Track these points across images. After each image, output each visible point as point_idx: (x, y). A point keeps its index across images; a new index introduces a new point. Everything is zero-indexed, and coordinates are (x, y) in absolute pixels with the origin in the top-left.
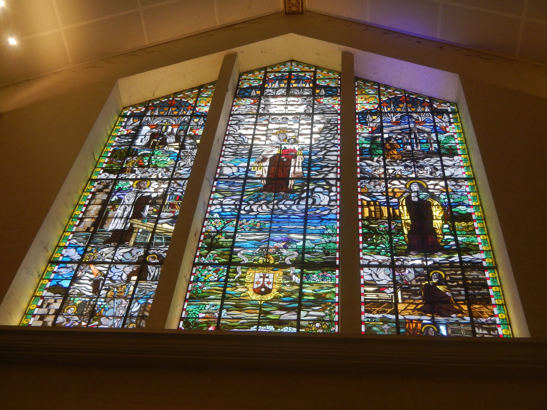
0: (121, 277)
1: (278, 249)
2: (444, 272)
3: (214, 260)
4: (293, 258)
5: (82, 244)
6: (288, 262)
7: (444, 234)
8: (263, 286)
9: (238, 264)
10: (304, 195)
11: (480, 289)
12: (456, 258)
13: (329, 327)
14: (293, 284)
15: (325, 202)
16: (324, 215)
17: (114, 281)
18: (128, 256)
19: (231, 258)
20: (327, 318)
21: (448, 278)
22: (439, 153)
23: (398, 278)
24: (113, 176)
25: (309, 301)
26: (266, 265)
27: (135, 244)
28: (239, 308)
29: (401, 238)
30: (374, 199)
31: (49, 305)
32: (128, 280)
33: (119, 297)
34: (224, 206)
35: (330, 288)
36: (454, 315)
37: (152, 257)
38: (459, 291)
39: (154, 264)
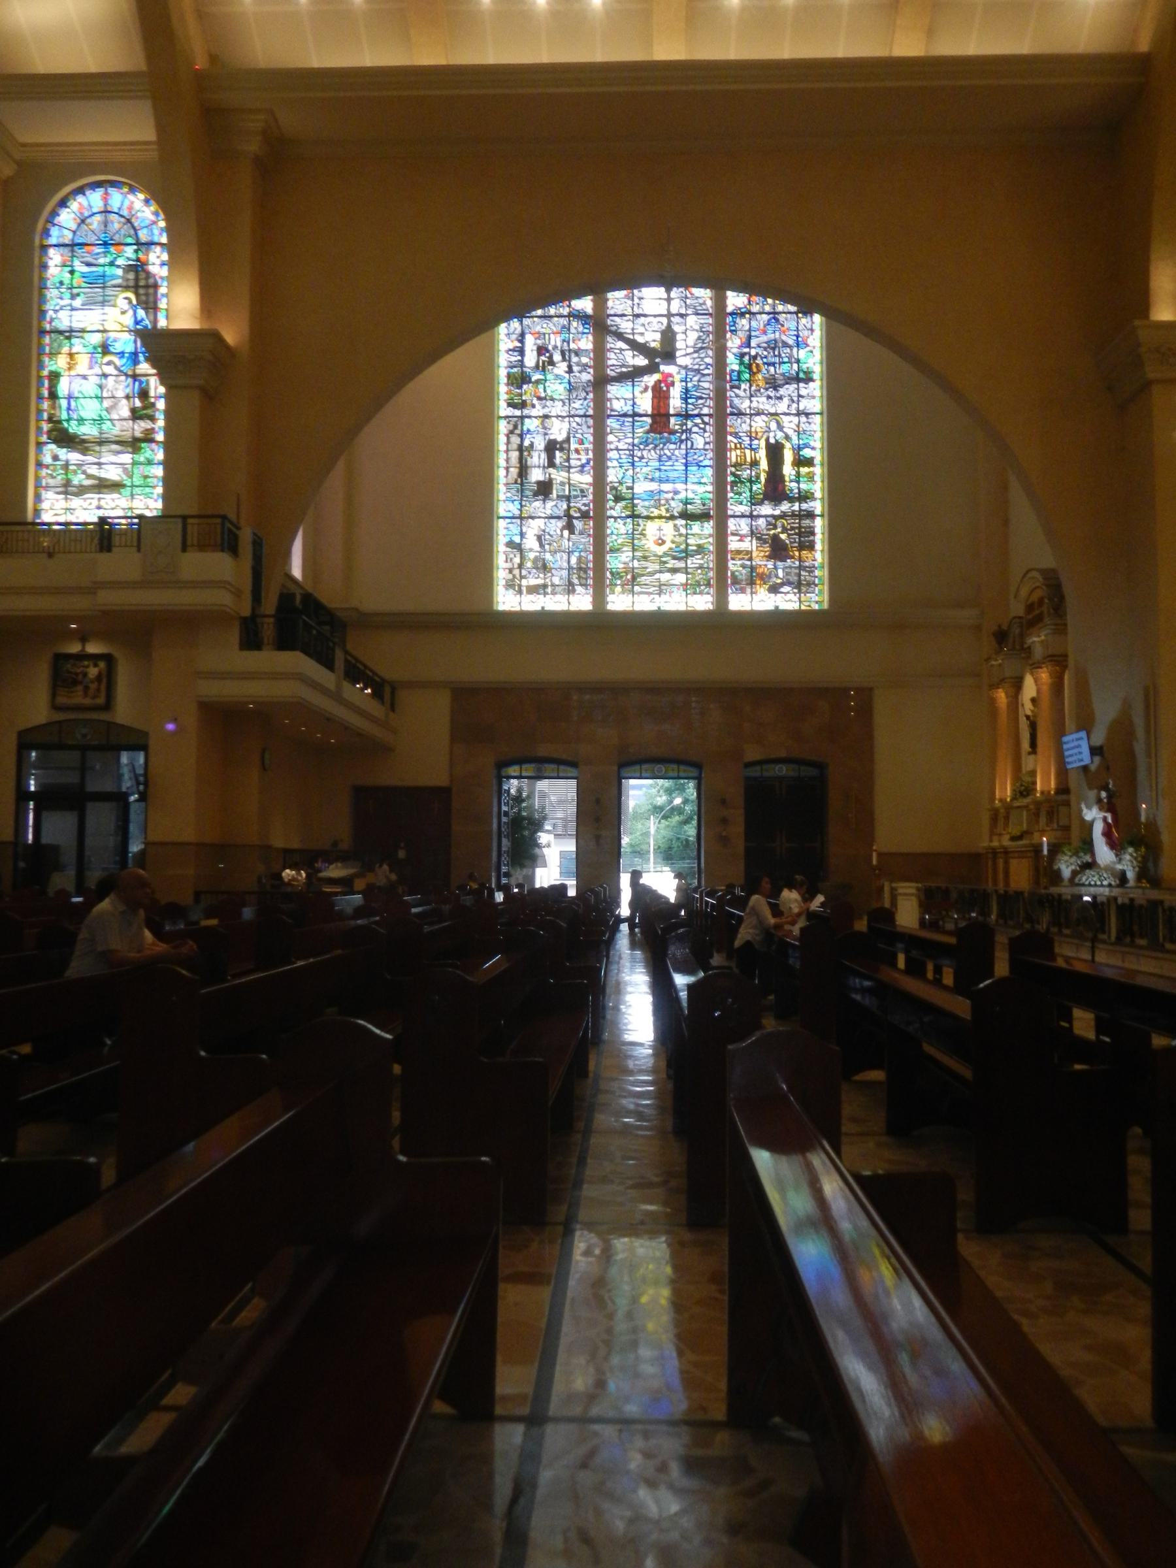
0: (555, 531)
1: (667, 500)
2: (786, 520)
3: (622, 512)
4: (679, 509)
5: (516, 498)
6: (676, 514)
7: (791, 481)
8: (660, 539)
9: (639, 516)
10: (684, 437)
11: (808, 537)
12: (796, 507)
13: (707, 573)
14: (681, 535)
15: (701, 446)
16: (701, 461)
17: (551, 536)
18: (555, 509)
19: (634, 511)
20: (706, 565)
21: (789, 527)
22: (797, 380)
23: (754, 528)
24: (518, 413)
25: (693, 551)
26: (660, 517)
27: (558, 496)
28: (645, 558)
29: (759, 486)
30: (740, 441)
31: (511, 560)
32: (562, 536)
33: (560, 551)
34: (620, 452)
35: (707, 538)
36: (788, 560)
37: (575, 511)
38: (795, 539)
39: (577, 518)
